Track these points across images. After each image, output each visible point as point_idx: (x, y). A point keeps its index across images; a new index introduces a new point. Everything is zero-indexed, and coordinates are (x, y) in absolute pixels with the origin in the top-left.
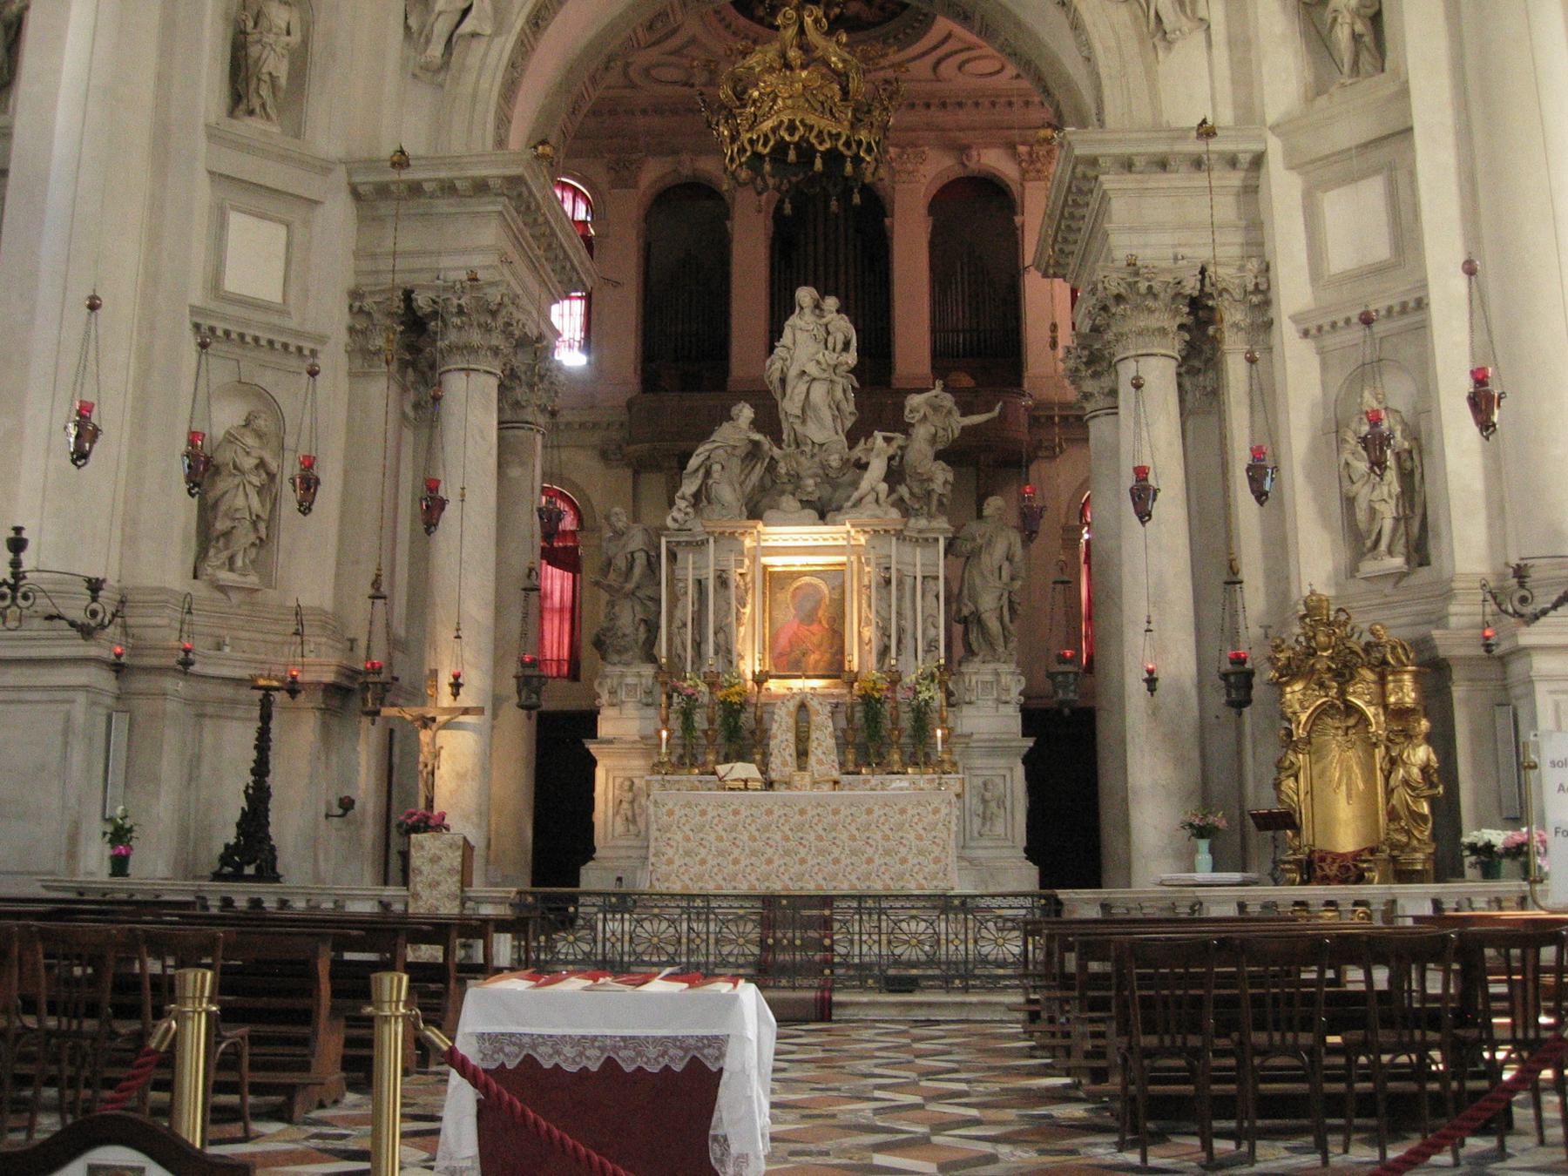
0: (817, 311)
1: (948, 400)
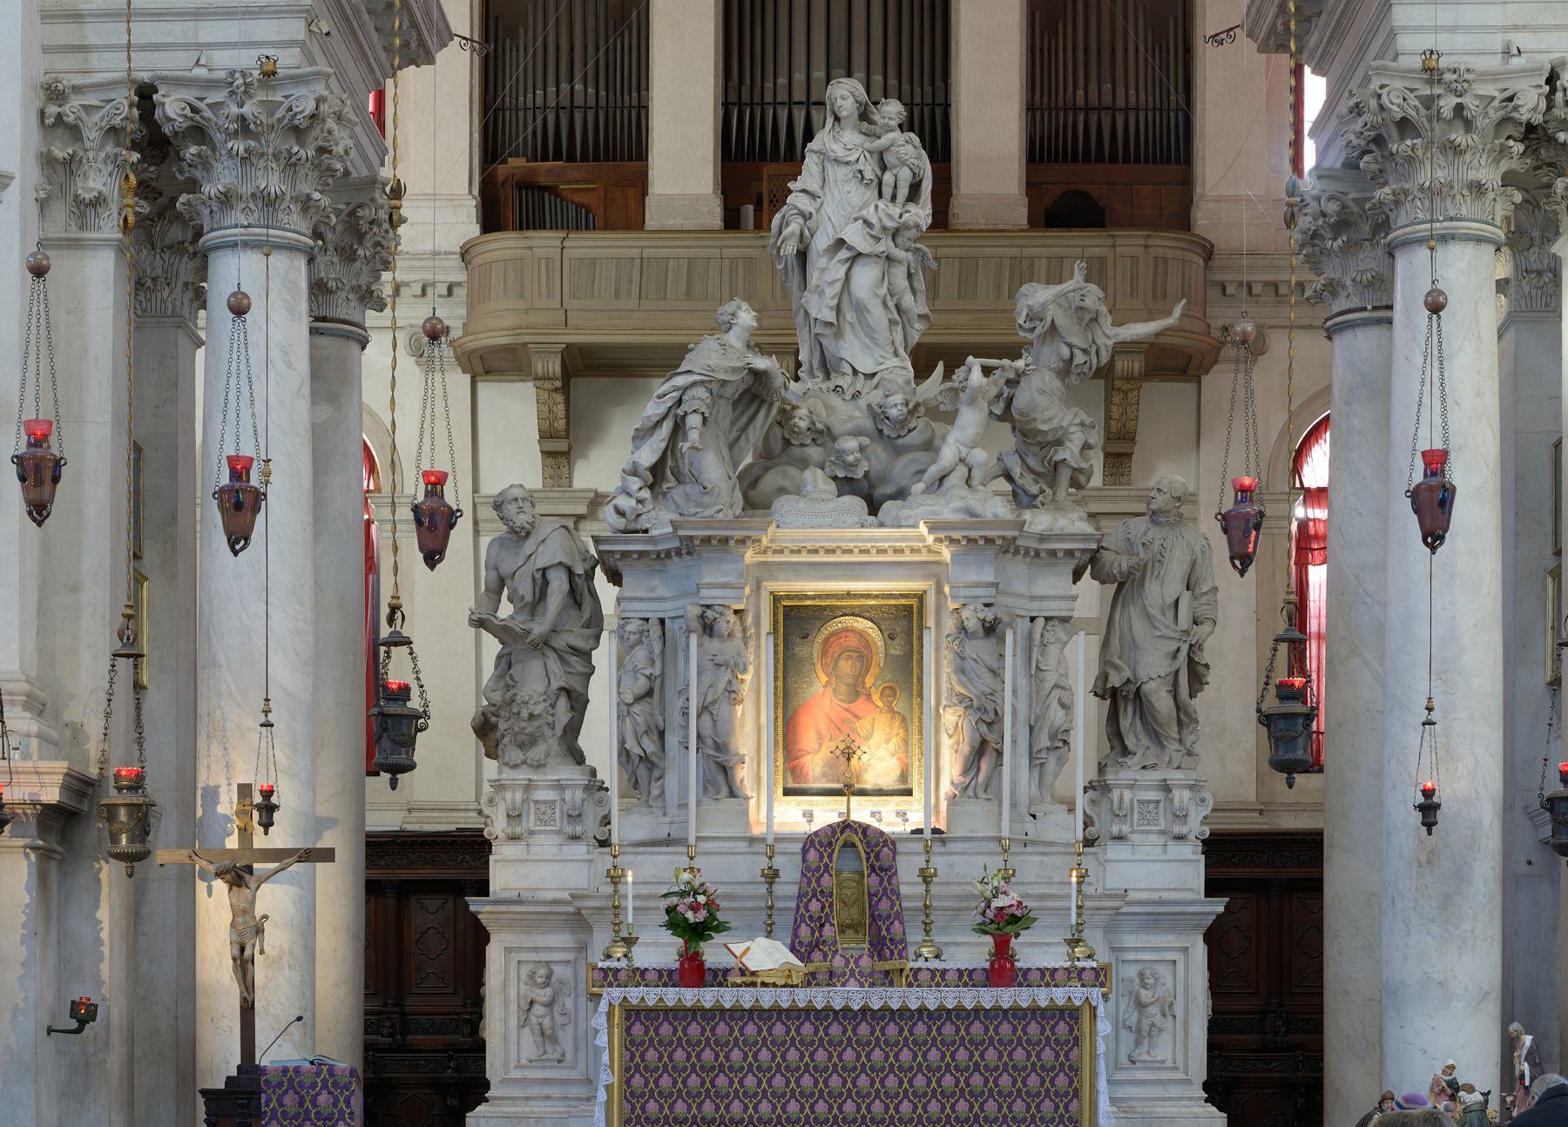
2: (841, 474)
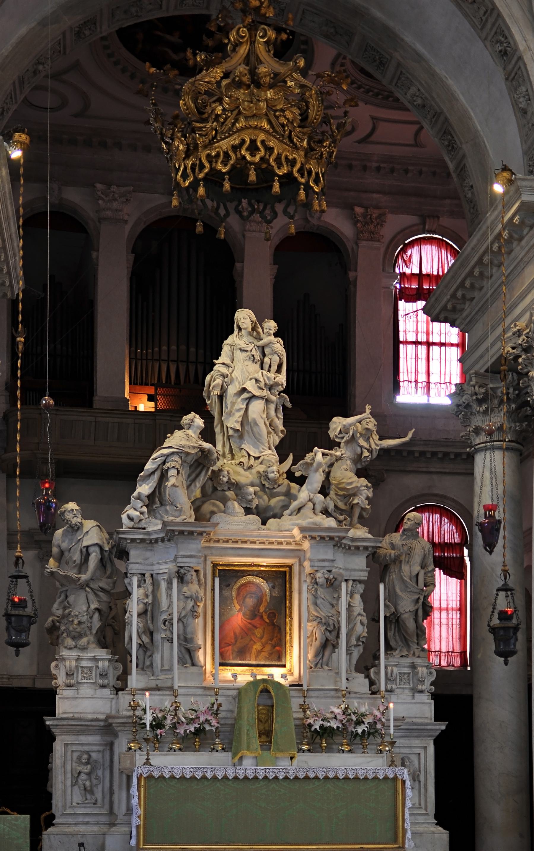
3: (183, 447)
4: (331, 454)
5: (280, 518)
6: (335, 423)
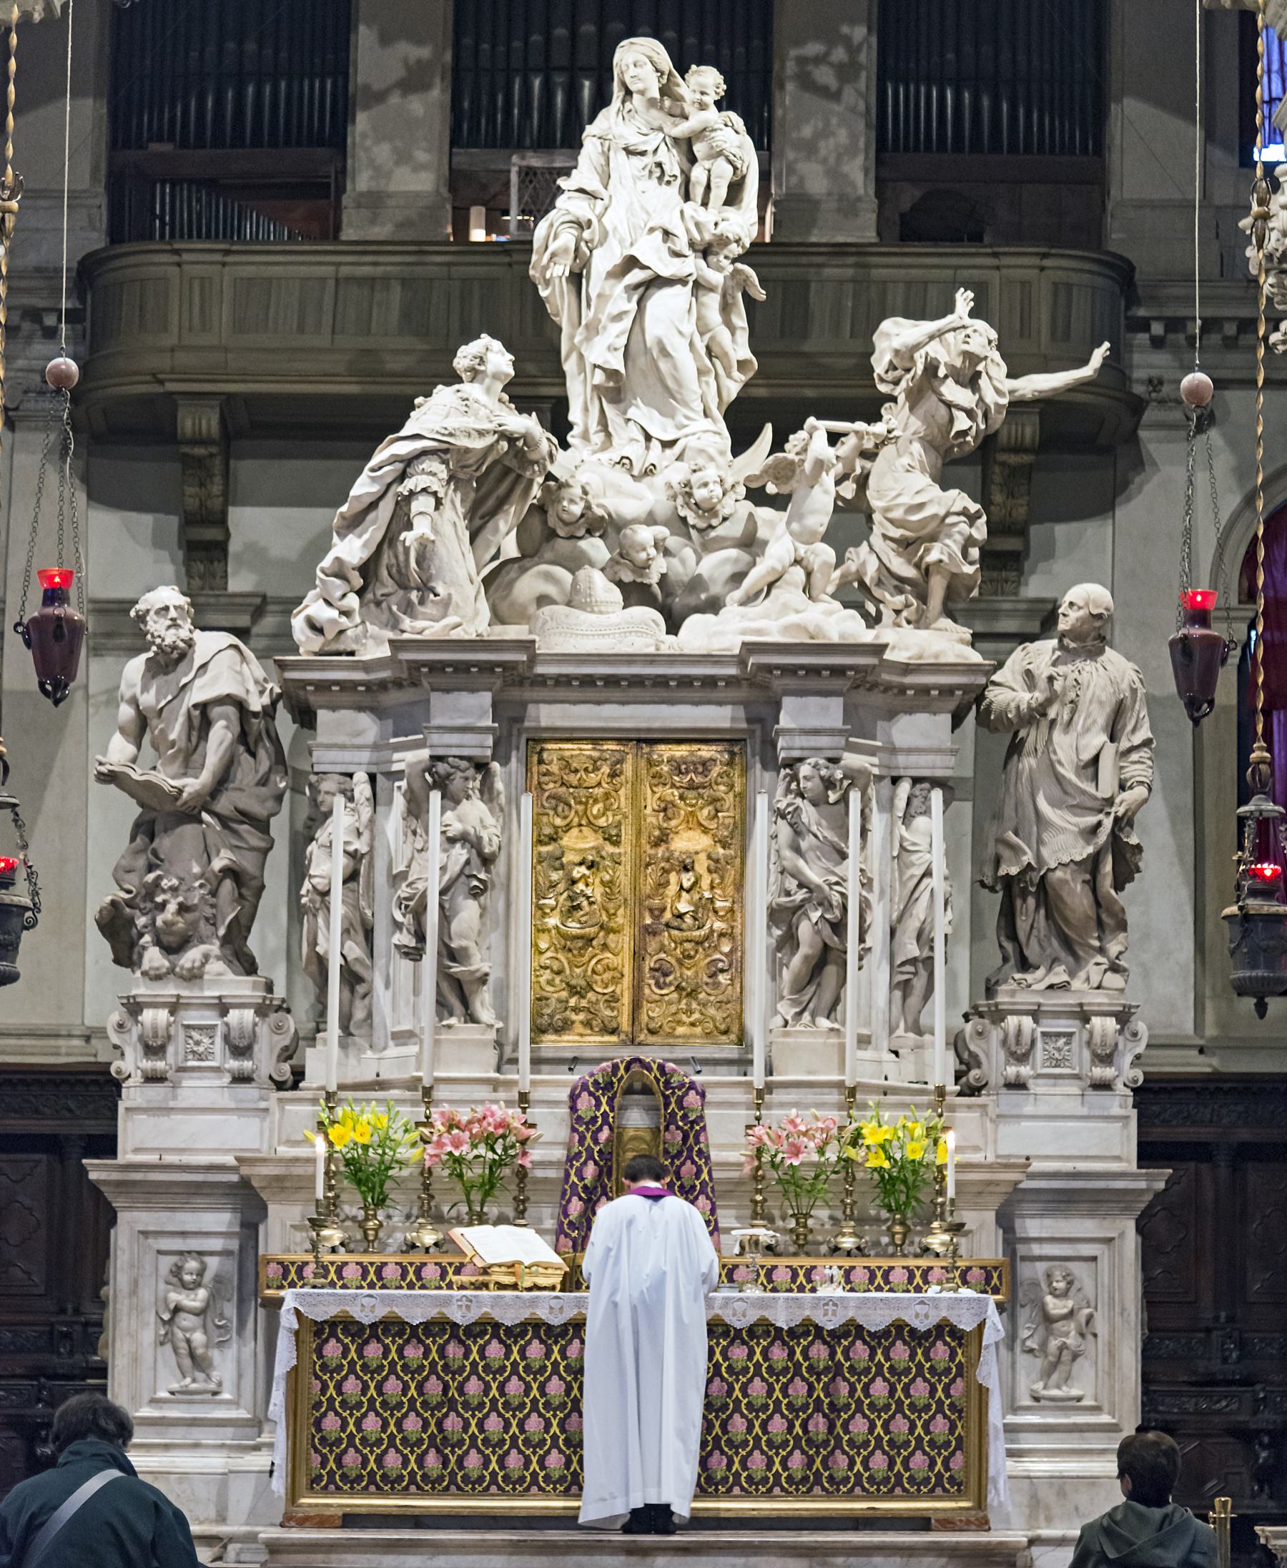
0: (667, 103)
1: (982, 336)
2: (627, 577)
3: (451, 435)
4: (857, 432)
5: (716, 613)
6: (888, 335)
